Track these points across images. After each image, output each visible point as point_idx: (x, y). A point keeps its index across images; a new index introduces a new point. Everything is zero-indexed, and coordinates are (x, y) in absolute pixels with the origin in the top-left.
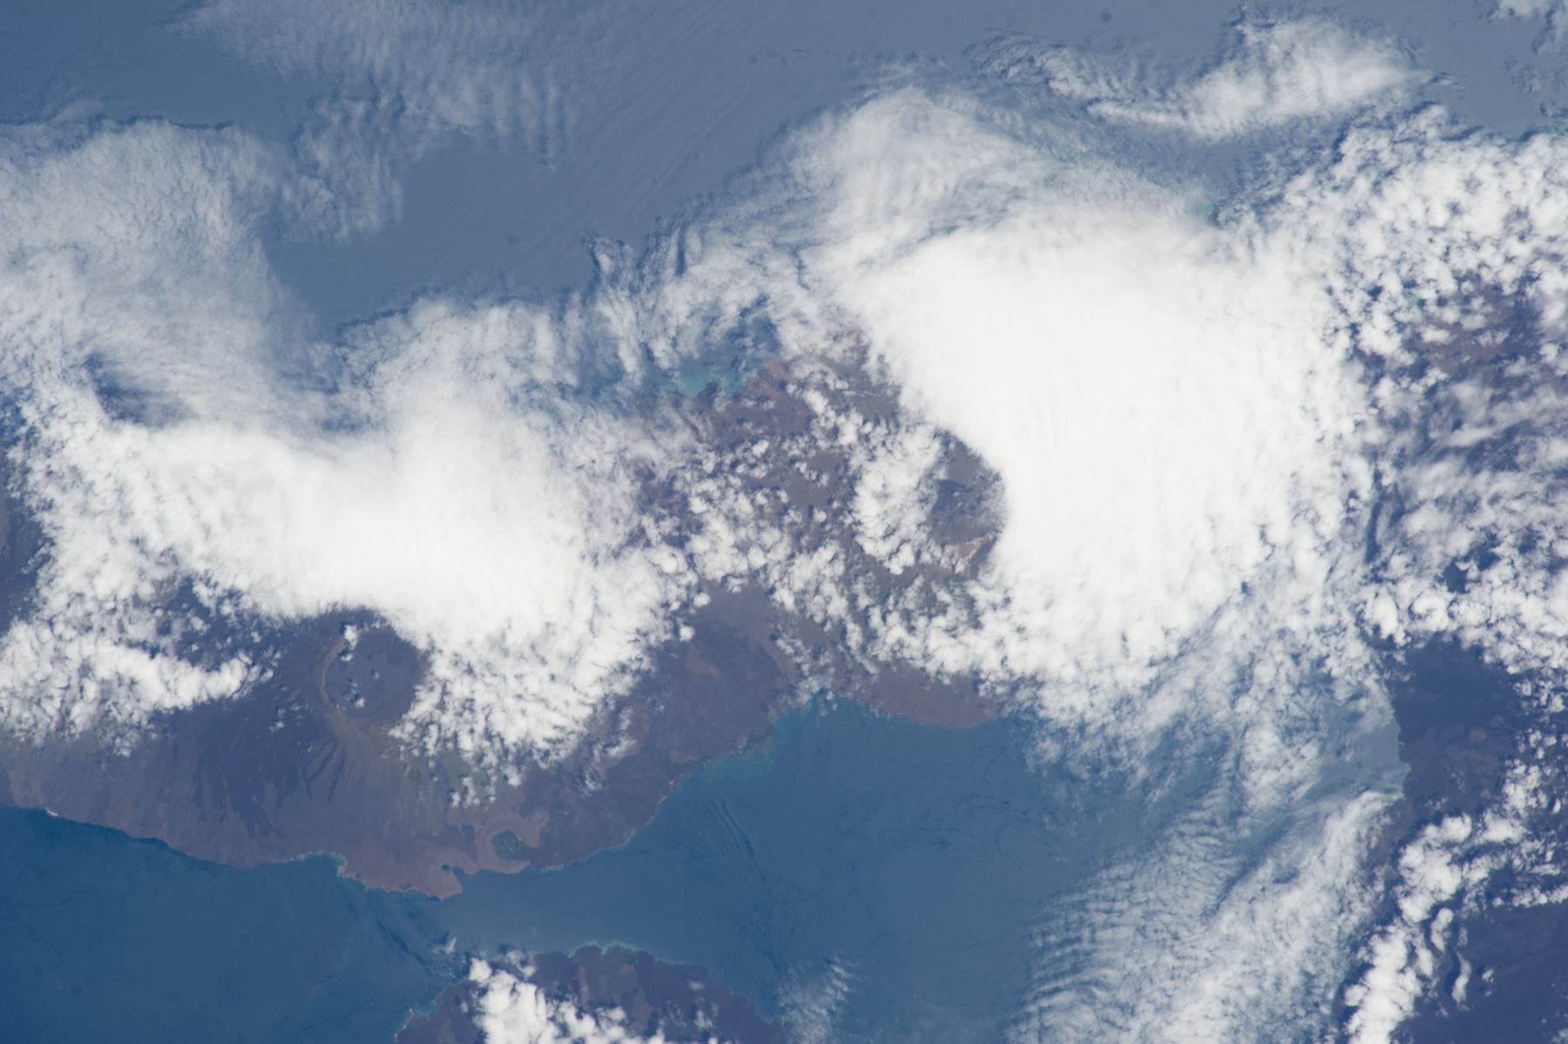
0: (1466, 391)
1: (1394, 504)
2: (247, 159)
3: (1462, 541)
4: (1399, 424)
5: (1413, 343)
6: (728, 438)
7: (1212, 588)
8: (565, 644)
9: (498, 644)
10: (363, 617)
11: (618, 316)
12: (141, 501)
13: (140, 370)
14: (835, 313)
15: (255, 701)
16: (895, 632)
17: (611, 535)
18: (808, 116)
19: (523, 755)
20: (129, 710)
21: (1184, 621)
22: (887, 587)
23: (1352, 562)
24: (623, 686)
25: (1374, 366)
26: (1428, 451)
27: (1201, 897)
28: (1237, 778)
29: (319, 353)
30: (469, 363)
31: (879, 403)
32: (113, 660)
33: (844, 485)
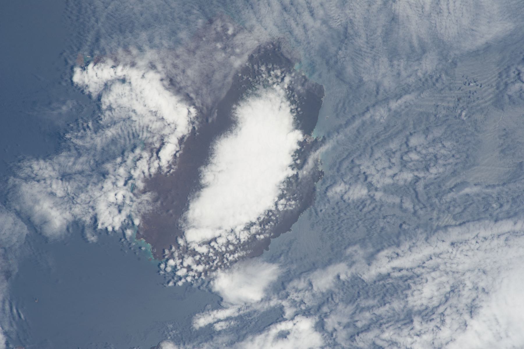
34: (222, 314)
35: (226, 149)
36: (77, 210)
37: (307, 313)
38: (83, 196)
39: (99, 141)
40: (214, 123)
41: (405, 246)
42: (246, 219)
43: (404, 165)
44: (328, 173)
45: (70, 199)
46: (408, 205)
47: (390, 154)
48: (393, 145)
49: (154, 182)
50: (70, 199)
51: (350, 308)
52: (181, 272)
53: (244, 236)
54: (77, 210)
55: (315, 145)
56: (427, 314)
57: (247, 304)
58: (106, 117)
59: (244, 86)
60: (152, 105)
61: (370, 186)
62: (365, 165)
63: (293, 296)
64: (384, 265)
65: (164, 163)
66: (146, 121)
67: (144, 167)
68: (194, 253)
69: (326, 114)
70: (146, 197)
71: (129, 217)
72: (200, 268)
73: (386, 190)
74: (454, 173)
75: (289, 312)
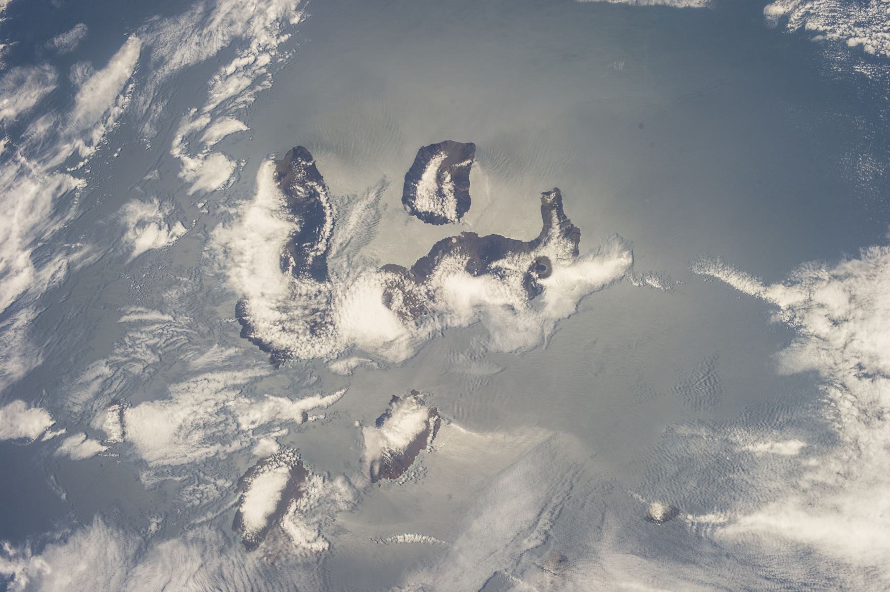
0: (319, 320)
1: (328, 303)
2: (492, 348)
3: (319, 297)
4: (328, 315)
5: (326, 327)
6: (422, 308)
7: (353, 289)
8: (445, 274)
9: (455, 273)
10: (474, 276)
11: (438, 326)
12: (508, 292)
13: (508, 313)
14: (407, 328)
15: (490, 262)
16: (397, 278)
17: (438, 291)
18: (412, 358)
19: (451, 255)
20: (509, 258)
21: (356, 283)
22: (398, 286)
23: (333, 294)
24: (436, 268)
25: (331, 324)
26: (324, 311)
27: (353, 240)
28: (349, 259)
29: (482, 318)
30: (460, 317)
31: (400, 314)
32: (512, 266)
33: (404, 301)
34: (276, 434)
35: (271, 508)
36: (331, 486)
37: (243, 432)
38: (328, 492)
39: (320, 516)
40: (274, 519)
41: (204, 457)
42: (264, 475)
43: (202, 493)
44: (232, 492)
45: (333, 491)
46: (202, 475)
47: (207, 498)
48: (205, 501)
49: (299, 495)
50: (333, 491)
51: (226, 432)
52: (291, 454)
53: (265, 467)
54: (331, 486)
55: (236, 505)
56: (198, 427)
57: (266, 437)
58: (316, 526)
59: (262, 534)
60: (298, 530)
61: (216, 485)
62: (217, 494)
63: (248, 440)
64: (212, 450)
65: (294, 503)
66: (301, 523)
67: (303, 502)
68: (285, 462)
69: (231, 518)
70: (302, 489)
71: (310, 480)
72: (283, 455)
73: (210, 483)
74: (184, 487)
75: (250, 432)
